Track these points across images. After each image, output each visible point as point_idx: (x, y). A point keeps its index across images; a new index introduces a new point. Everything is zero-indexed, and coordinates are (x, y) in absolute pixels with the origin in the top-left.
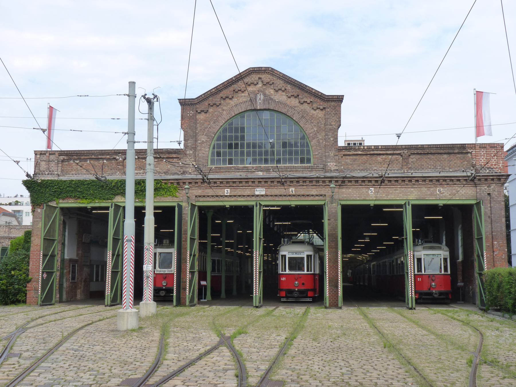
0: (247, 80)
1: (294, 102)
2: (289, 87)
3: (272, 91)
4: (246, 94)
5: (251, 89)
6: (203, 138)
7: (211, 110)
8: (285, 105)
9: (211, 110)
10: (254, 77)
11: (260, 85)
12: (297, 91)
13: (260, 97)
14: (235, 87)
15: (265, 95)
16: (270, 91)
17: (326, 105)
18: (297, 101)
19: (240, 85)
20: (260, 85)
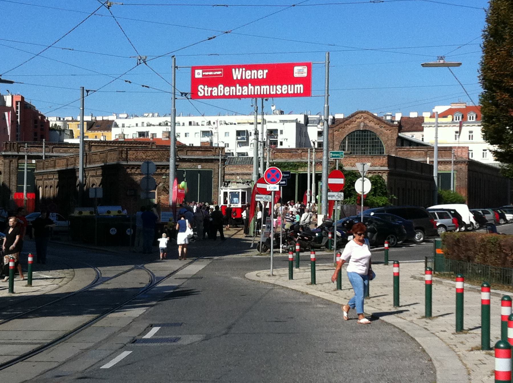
0: (356, 116)
1: (377, 127)
2: (375, 120)
3: (368, 122)
4: (356, 122)
5: (358, 120)
6: (336, 143)
7: (340, 130)
8: (373, 128)
9: (340, 130)
10: (360, 115)
11: (362, 118)
12: (378, 122)
13: (362, 124)
14: (351, 119)
15: (364, 123)
16: (367, 121)
17: (392, 128)
18: (379, 126)
19: (354, 119)
20: (362, 118)
